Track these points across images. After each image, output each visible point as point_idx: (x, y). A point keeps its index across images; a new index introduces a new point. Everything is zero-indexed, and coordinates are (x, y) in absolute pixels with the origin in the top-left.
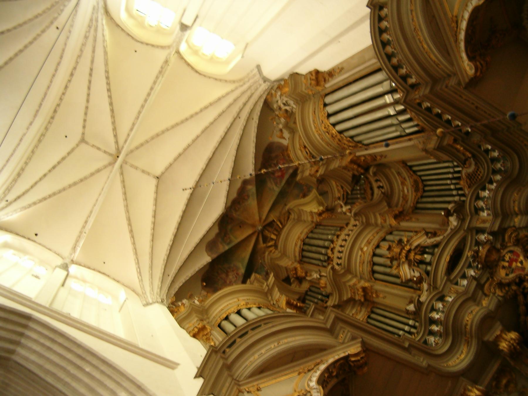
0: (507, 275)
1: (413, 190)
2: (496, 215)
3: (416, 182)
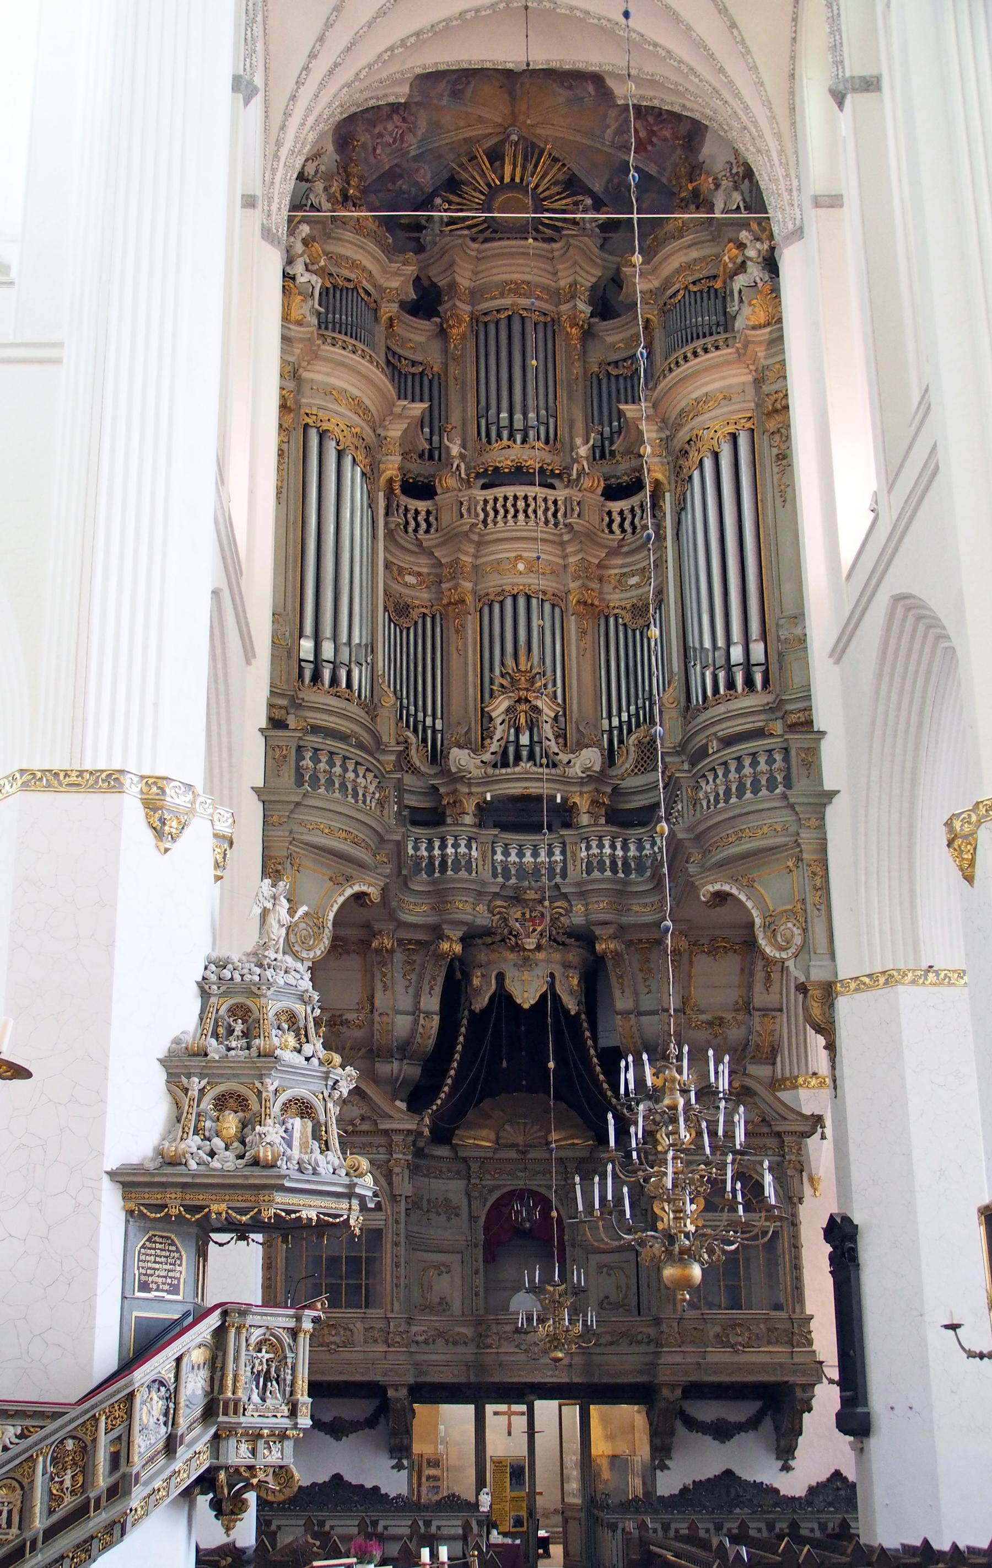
0: (517, 920)
2: (578, 884)
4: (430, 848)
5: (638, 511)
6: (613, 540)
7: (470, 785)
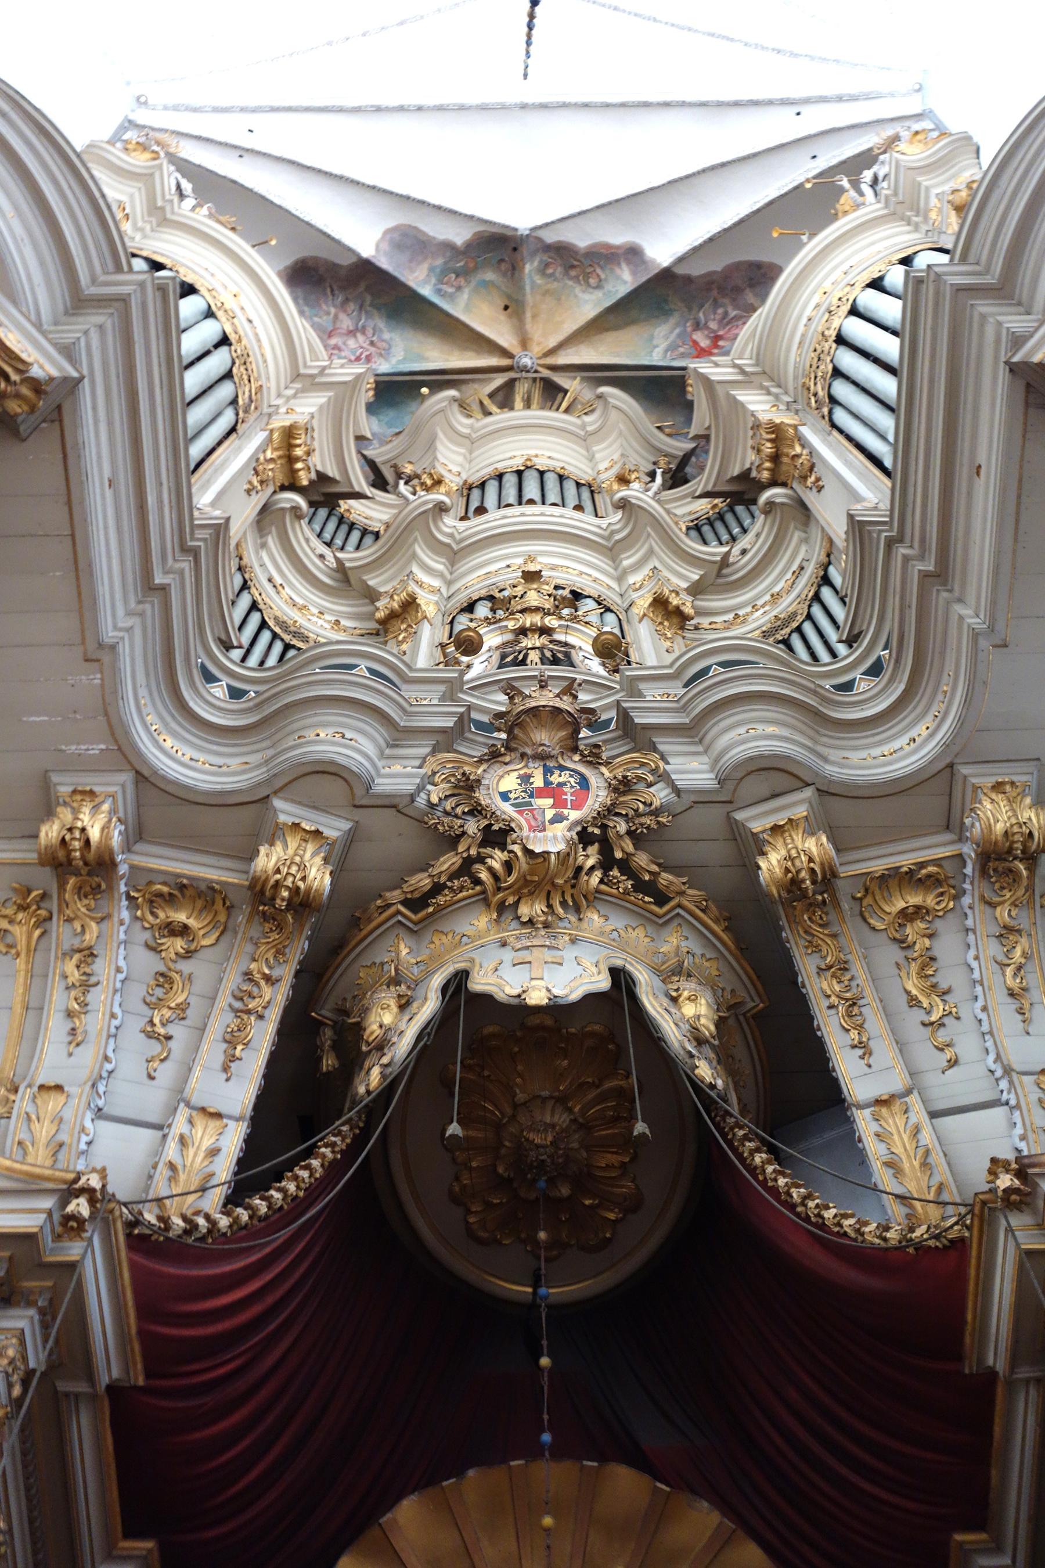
0: (505, 796)
3: (793, 616)
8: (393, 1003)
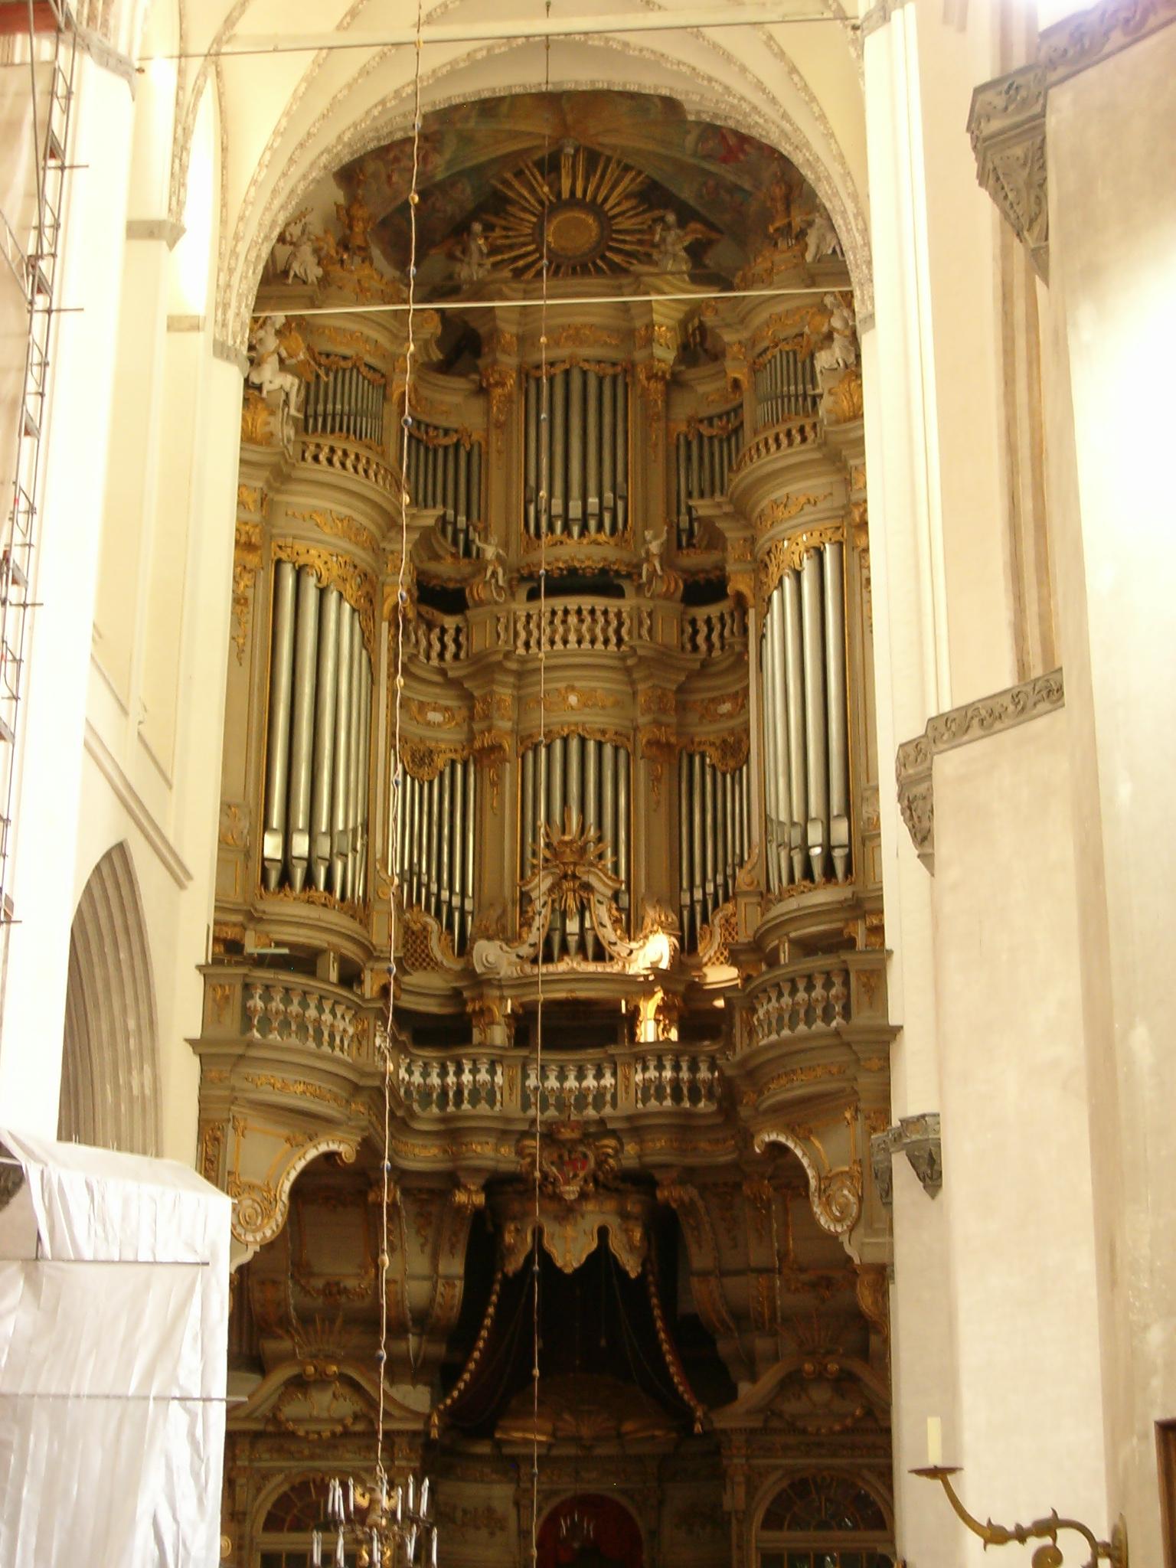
1: (725, 735)
2: (629, 1118)
4: (443, 1074)
5: (727, 617)
6: (695, 660)
7: (500, 987)
8: (512, 1228)
